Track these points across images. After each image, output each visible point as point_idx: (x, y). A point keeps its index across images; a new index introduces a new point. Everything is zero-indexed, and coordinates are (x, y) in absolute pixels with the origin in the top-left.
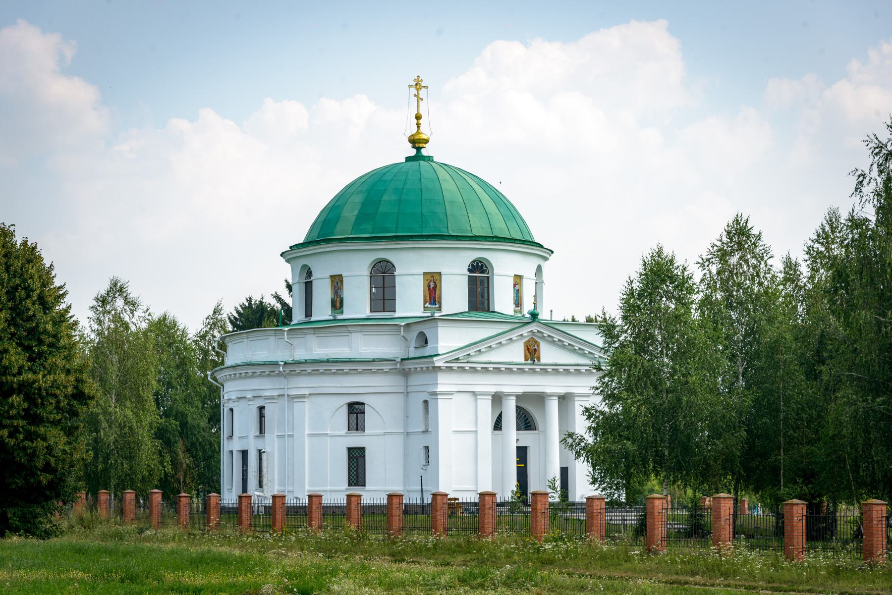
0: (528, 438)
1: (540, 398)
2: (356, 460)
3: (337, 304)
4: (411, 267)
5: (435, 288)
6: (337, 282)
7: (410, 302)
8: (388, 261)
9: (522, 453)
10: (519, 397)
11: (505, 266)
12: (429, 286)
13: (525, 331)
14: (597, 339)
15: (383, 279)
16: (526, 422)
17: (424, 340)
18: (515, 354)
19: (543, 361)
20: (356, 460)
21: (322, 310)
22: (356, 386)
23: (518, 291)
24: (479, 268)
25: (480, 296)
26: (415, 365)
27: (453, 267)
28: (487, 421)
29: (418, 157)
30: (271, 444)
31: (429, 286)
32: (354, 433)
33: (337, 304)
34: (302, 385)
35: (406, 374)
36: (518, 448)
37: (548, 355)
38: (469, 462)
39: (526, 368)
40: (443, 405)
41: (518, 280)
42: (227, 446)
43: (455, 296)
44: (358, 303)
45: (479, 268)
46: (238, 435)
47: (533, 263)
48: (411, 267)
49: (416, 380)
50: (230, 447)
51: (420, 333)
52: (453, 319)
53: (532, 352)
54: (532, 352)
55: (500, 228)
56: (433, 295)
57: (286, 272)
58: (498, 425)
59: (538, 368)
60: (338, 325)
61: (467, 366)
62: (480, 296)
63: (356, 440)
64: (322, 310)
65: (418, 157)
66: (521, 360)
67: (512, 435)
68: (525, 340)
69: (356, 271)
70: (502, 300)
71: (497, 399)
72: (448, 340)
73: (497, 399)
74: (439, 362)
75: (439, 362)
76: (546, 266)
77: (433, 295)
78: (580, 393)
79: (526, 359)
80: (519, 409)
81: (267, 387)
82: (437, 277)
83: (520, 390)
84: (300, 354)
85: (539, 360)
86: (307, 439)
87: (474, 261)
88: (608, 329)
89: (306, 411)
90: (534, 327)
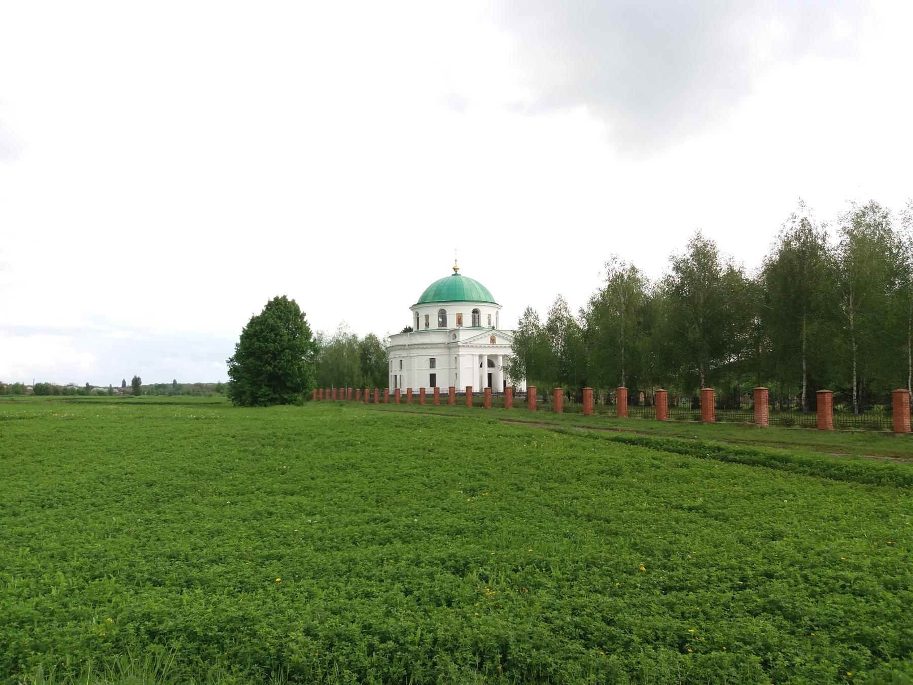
0: (491, 370)
1: (496, 356)
2: (433, 377)
3: (427, 325)
4: (452, 311)
6: (427, 317)
7: (452, 323)
9: (490, 375)
11: (485, 311)
13: (490, 333)
14: (510, 334)
15: (443, 315)
16: (491, 364)
17: (455, 336)
18: (487, 341)
20: (433, 377)
21: (422, 327)
22: (433, 353)
24: (475, 311)
25: (476, 323)
26: (452, 346)
27: (466, 312)
28: (478, 365)
29: (456, 274)
30: (404, 373)
33: (427, 325)
34: (414, 352)
35: (449, 348)
37: (498, 341)
38: (470, 377)
40: (461, 358)
42: (390, 374)
43: (467, 321)
44: (434, 323)
45: (475, 311)
46: (394, 370)
47: (495, 310)
48: (452, 311)
49: (453, 350)
50: (391, 374)
51: (454, 333)
52: (467, 329)
53: (493, 340)
54: (493, 340)
55: (483, 298)
56: (460, 321)
57: (411, 314)
58: (481, 366)
60: (427, 332)
62: (476, 323)
63: (433, 371)
64: (422, 327)
65: (456, 274)
67: (486, 370)
69: (433, 313)
70: (484, 323)
71: (481, 356)
72: (463, 336)
73: (481, 356)
74: (459, 344)
75: (459, 344)
76: (500, 311)
77: (460, 321)
78: (505, 351)
81: (403, 353)
84: (414, 342)
88: (514, 332)
89: (415, 361)
90: (493, 332)
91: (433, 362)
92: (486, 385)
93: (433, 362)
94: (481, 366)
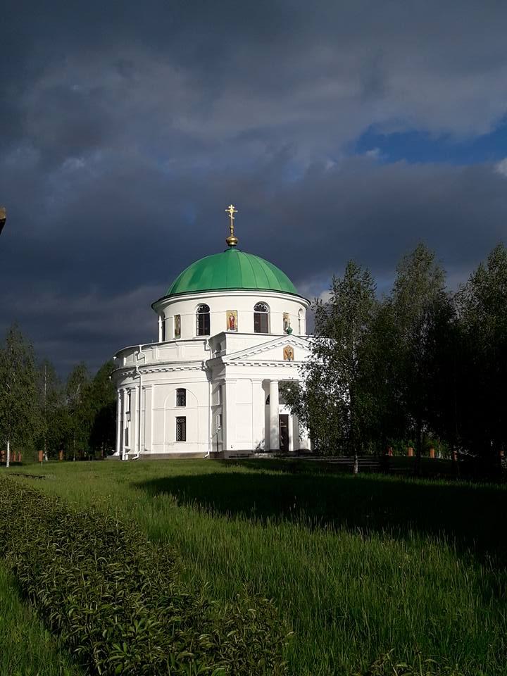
2: (181, 422)
3: (178, 333)
5: (234, 320)
7: (218, 325)
8: (206, 306)
10: (280, 383)
12: (230, 319)
18: (279, 354)
19: (295, 360)
20: (181, 422)
23: (286, 322)
31: (230, 319)
32: (181, 408)
33: (178, 333)
36: (280, 415)
39: (285, 363)
41: (285, 316)
43: (246, 322)
56: (232, 324)
59: (292, 364)
61: (245, 362)
63: (181, 412)
66: (282, 359)
68: (284, 346)
70: (276, 325)
71: (266, 384)
72: (232, 344)
77: (232, 324)
79: (285, 358)
80: (280, 390)
82: (234, 313)
83: (281, 378)
85: (293, 359)
86: (152, 411)
87: (258, 304)
90: (290, 338)
91: (181, 396)
92: (275, 445)
93: (181, 396)
94: (268, 401)
